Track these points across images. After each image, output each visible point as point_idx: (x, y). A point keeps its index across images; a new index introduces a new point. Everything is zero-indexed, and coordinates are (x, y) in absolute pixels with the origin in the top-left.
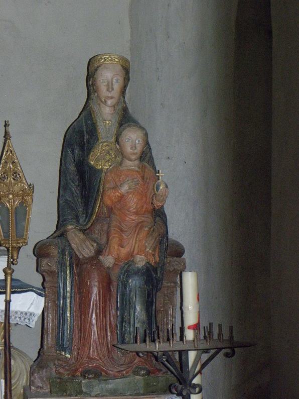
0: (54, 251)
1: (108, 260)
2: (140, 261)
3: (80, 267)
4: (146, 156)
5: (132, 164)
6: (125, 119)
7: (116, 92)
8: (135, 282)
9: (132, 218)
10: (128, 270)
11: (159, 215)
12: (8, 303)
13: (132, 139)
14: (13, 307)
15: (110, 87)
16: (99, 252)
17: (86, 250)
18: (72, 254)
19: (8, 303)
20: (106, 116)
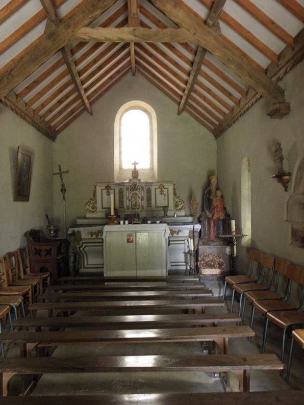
0: (204, 216)
1: (215, 218)
2: (222, 218)
3: (209, 220)
4: (222, 197)
5: (219, 198)
6: (218, 189)
7: (216, 183)
8: (220, 222)
9: (219, 209)
10: (219, 219)
11: (225, 208)
12: (194, 226)
13: (219, 193)
14: (195, 227)
15: (214, 182)
16: (213, 216)
17: (210, 216)
18: (207, 216)
19: (194, 226)
20: (213, 188)
